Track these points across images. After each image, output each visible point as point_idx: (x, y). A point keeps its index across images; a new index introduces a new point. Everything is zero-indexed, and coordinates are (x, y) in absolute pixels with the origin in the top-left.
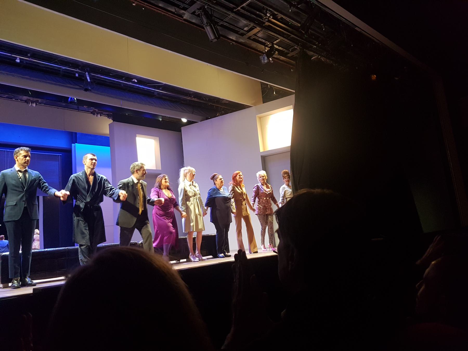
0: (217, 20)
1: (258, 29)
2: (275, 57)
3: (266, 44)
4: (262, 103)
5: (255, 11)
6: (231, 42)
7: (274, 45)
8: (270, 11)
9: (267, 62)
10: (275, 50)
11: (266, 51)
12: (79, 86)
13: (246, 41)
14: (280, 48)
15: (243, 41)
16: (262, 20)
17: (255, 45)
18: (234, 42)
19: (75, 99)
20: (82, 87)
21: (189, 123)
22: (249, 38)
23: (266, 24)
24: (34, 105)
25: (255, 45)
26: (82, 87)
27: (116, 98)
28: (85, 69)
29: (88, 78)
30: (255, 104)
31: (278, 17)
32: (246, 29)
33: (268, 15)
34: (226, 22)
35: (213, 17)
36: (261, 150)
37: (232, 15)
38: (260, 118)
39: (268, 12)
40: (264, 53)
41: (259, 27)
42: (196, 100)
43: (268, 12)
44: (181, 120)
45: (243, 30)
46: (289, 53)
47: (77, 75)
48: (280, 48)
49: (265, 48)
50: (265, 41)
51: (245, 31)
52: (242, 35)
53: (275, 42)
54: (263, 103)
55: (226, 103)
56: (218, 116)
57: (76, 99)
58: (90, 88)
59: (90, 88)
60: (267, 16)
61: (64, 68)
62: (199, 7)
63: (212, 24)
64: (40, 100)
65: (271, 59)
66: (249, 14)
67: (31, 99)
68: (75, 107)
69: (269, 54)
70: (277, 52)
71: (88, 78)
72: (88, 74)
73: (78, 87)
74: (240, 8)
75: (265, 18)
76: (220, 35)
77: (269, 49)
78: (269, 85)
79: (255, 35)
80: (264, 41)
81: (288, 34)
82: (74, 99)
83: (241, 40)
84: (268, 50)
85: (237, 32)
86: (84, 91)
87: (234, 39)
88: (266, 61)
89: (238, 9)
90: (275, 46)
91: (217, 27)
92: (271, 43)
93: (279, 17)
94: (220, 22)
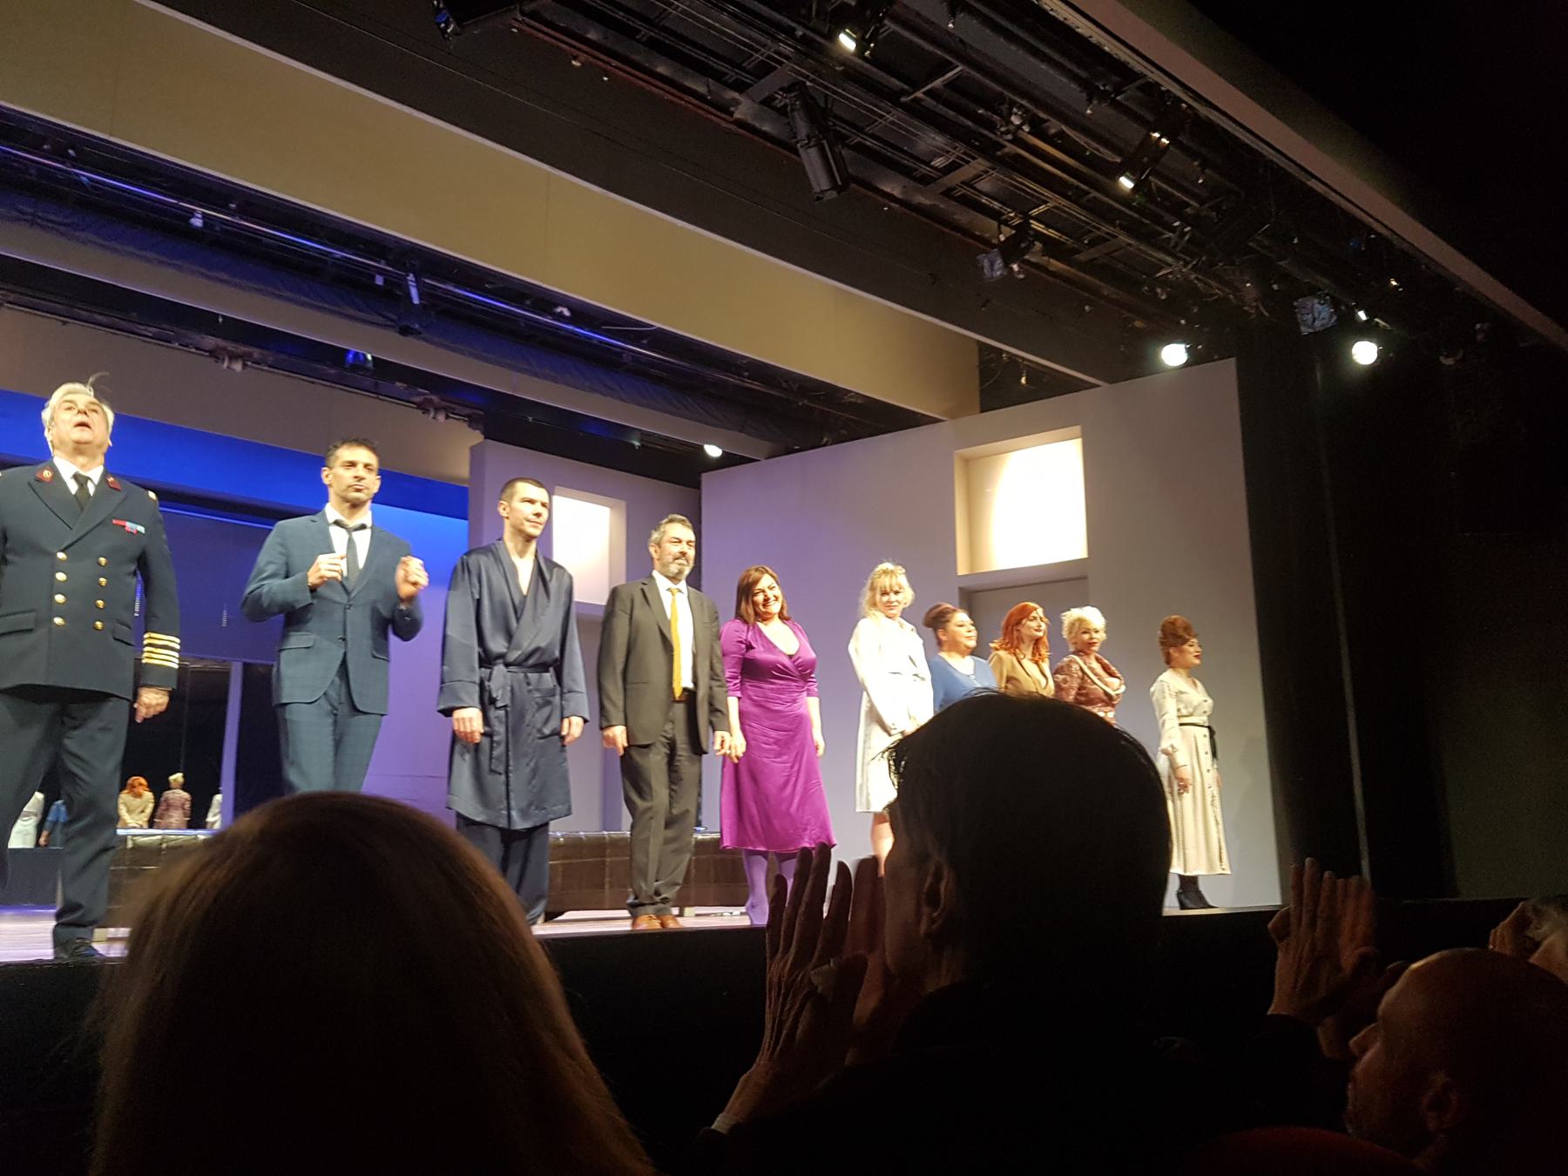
0: (844, 129)
1: (980, 164)
2: (1032, 263)
3: (1004, 217)
4: (978, 410)
5: (972, 106)
6: (886, 201)
7: (1031, 221)
8: (1021, 107)
9: (1001, 275)
10: (1031, 239)
11: (1002, 238)
12: (384, 317)
13: (937, 203)
14: (1052, 233)
15: (928, 202)
16: (992, 136)
17: (963, 216)
18: (896, 203)
19: (369, 357)
20: (392, 321)
21: (728, 461)
22: (947, 193)
23: (1006, 150)
24: (238, 366)
25: (963, 216)
26: (392, 321)
27: (500, 364)
28: (405, 264)
29: (414, 292)
30: (954, 414)
31: (1048, 128)
32: (938, 162)
33: (1016, 121)
34: (873, 136)
35: (830, 119)
36: (962, 570)
37: (893, 116)
38: (967, 461)
39: (1015, 110)
40: (994, 246)
41: (984, 158)
42: (756, 386)
43: (1015, 110)
44: (701, 448)
45: (928, 164)
46: (1078, 251)
47: (379, 281)
48: (1052, 233)
49: (999, 228)
50: (1000, 205)
51: (936, 169)
52: (925, 180)
53: (1035, 212)
54: (982, 412)
55: (855, 403)
56: (825, 445)
57: (373, 357)
58: (417, 326)
59: (417, 326)
60: (1012, 123)
61: (339, 254)
62: (786, 85)
63: (825, 142)
64: (256, 353)
65: (1015, 267)
66: (951, 113)
67: (231, 346)
68: (368, 382)
69: (1011, 251)
70: (1038, 245)
71: (414, 292)
72: (413, 279)
73: (380, 319)
74: (924, 93)
75: (1002, 129)
76: (848, 179)
77: (1014, 232)
78: (1007, 353)
79: (968, 184)
80: (996, 205)
81: (1078, 187)
82: (365, 356)
83: (921, 199)
84: (1008, 235)
85: (906, 172)
86: (398, 334)
87: (897, 193)
88: (998, 273)
89: (916, 97)
90: (1036, 225)
91: (840, 153)
92: (1021, 213)
93: (1053, 131)
94: (854, 136)
